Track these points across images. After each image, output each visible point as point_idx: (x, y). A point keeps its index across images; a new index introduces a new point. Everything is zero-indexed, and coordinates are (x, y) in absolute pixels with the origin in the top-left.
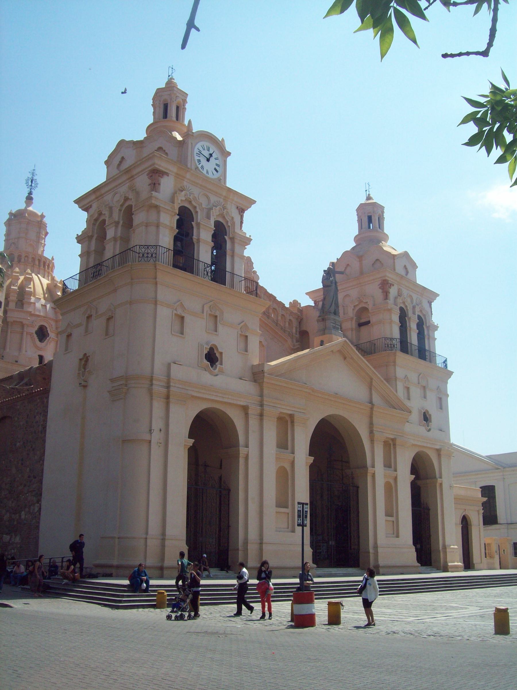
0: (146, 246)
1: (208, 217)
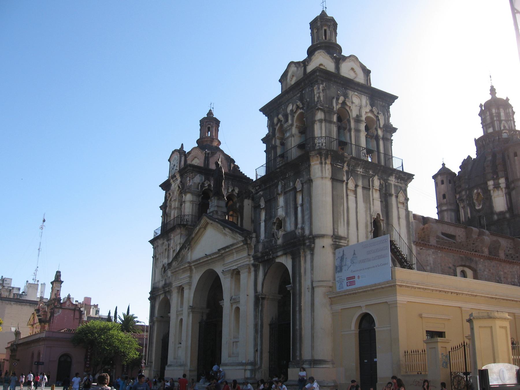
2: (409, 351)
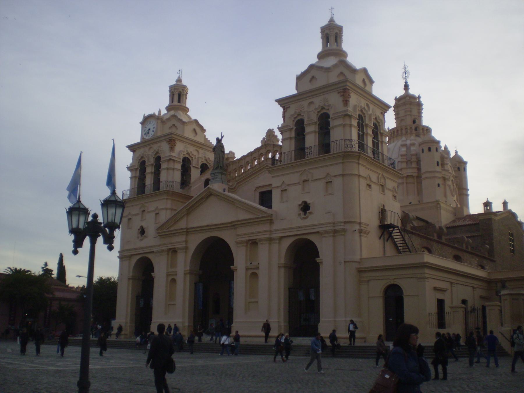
1: (370, 120)
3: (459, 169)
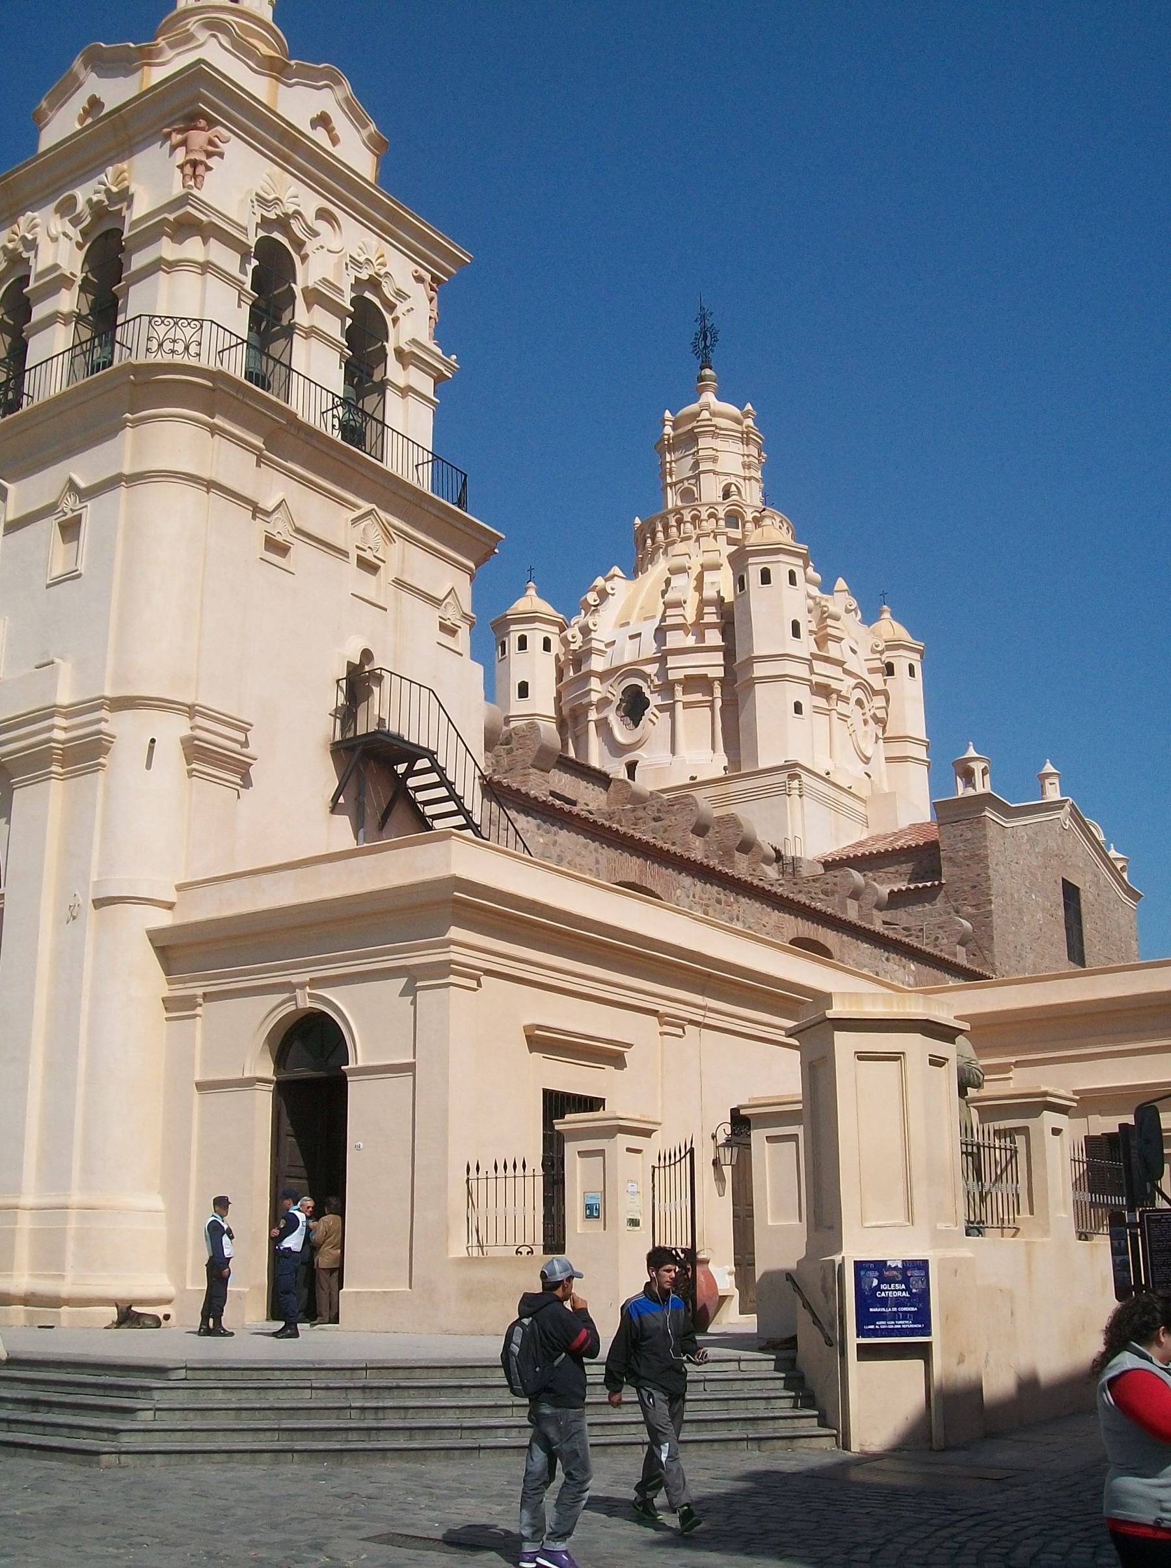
0: (169, 320)
2: (487, 1167)
3: (889, 669)
